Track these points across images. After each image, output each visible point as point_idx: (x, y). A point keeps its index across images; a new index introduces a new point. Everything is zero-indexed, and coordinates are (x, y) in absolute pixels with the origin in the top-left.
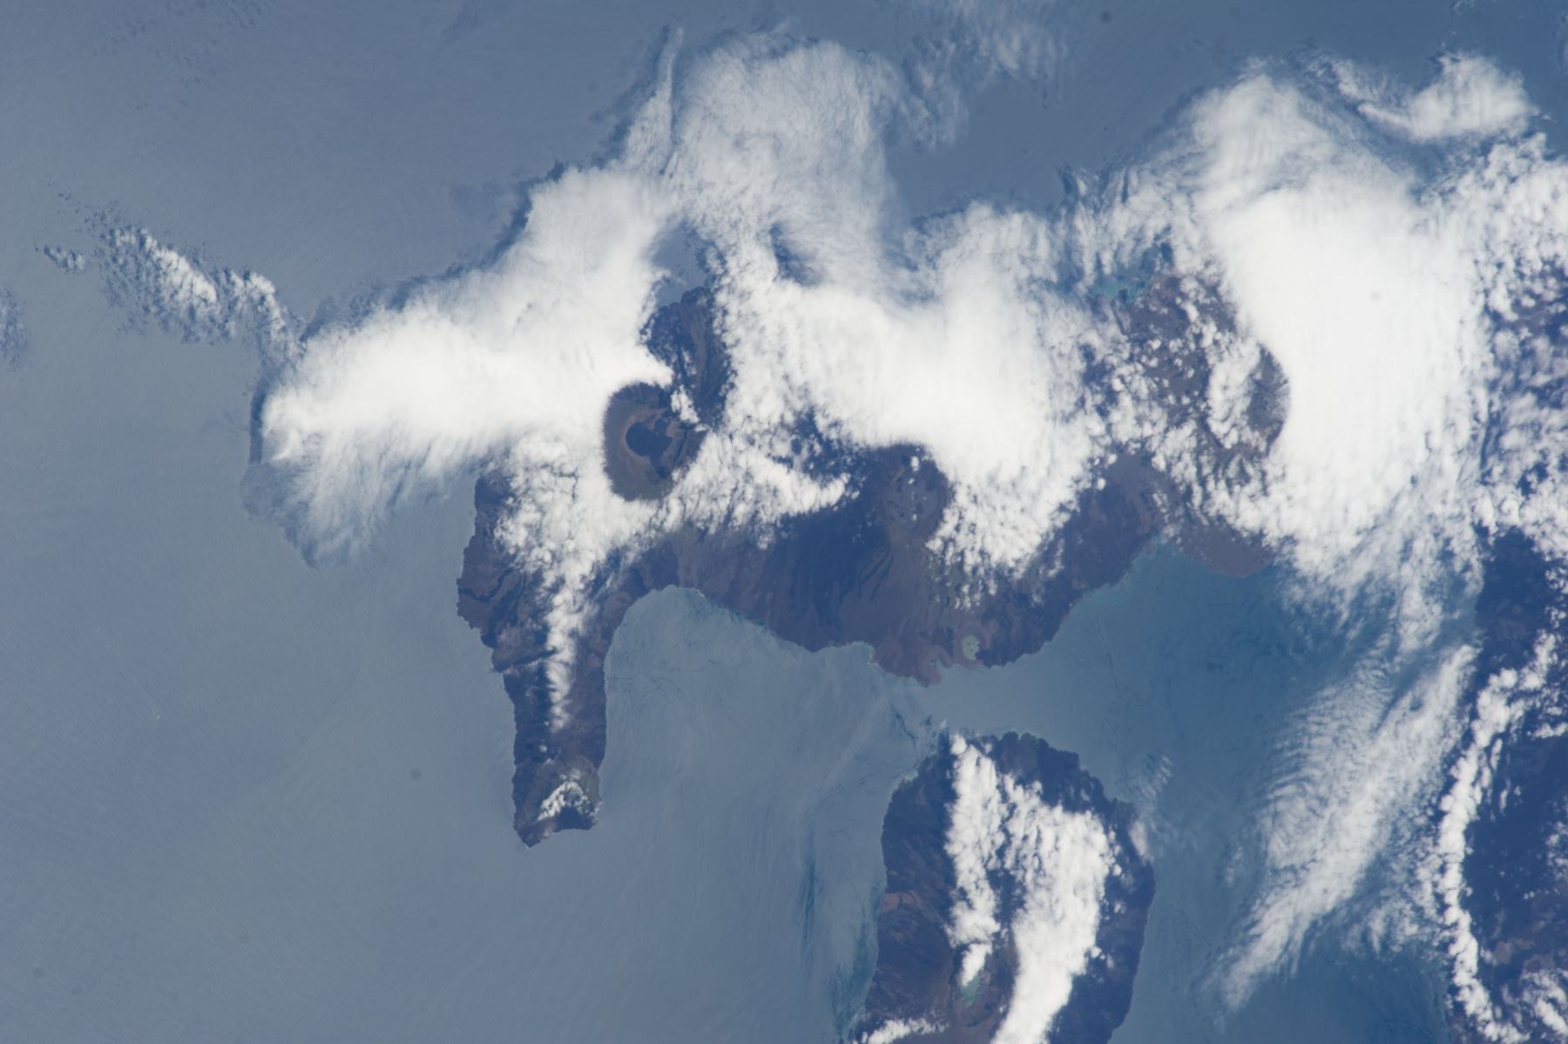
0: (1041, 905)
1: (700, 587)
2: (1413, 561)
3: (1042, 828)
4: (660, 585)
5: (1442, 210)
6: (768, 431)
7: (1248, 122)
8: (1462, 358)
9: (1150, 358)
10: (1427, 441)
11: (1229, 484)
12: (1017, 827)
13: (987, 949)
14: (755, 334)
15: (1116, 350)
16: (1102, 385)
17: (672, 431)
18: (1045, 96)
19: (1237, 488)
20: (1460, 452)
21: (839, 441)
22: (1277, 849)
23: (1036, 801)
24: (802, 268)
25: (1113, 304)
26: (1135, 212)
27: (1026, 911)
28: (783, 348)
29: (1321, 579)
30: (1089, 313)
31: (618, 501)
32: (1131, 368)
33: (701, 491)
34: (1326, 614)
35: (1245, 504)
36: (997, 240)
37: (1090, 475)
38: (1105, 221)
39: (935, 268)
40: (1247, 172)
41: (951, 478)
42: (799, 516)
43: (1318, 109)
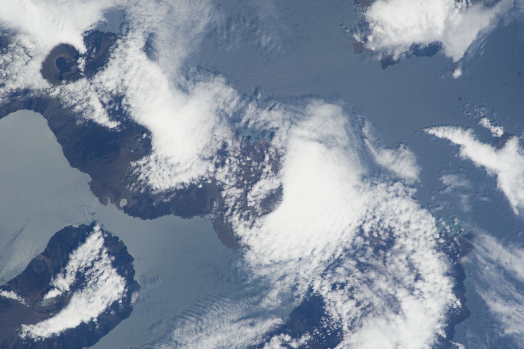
0: (88, 293)
1: (49, 121)
2: (283, 282)
3: (105, 271)
4: (36, 111)
5: (368, 188)
6: (104, 91)
7: (325, 117)
8: (342, 235)
9: (244, 161)
10: (313, 251)
11: (241, 216)
12: (97, 265)
13: (60, 293)
14: (122, 60)
15: (235, 151)
16: (223, 158)
17: (73, 68)
18: (268, 62)
19: (242, 219)
20: (321, 262)
21: (126, 112)
23: (109, 262)
24: (152, 52)
25: (243, 137)
26: (270, 116)
27: (82, 291)
28: (128, 71)
29: (249, 266)
30: (234, 134)
31: (40, 76)
32: (235, 160)
33: (69, 93)
34: (244, 277)
35: (241, 226)
36: (221, 91)
37: (199, 181)
38: (259, 111)
39: (194, 84)
40: (315, 131)
41: (153, 148)
42: (96, 124)
43: (351, 130)
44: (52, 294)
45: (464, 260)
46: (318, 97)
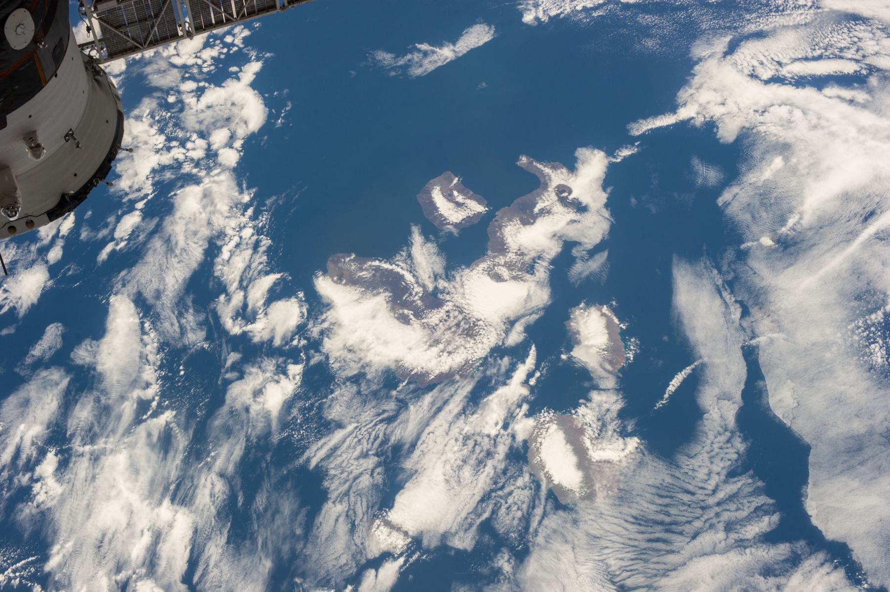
22: (429, 245)
44: (455, 193)
45: (457, 377)
46: (551, 292)
